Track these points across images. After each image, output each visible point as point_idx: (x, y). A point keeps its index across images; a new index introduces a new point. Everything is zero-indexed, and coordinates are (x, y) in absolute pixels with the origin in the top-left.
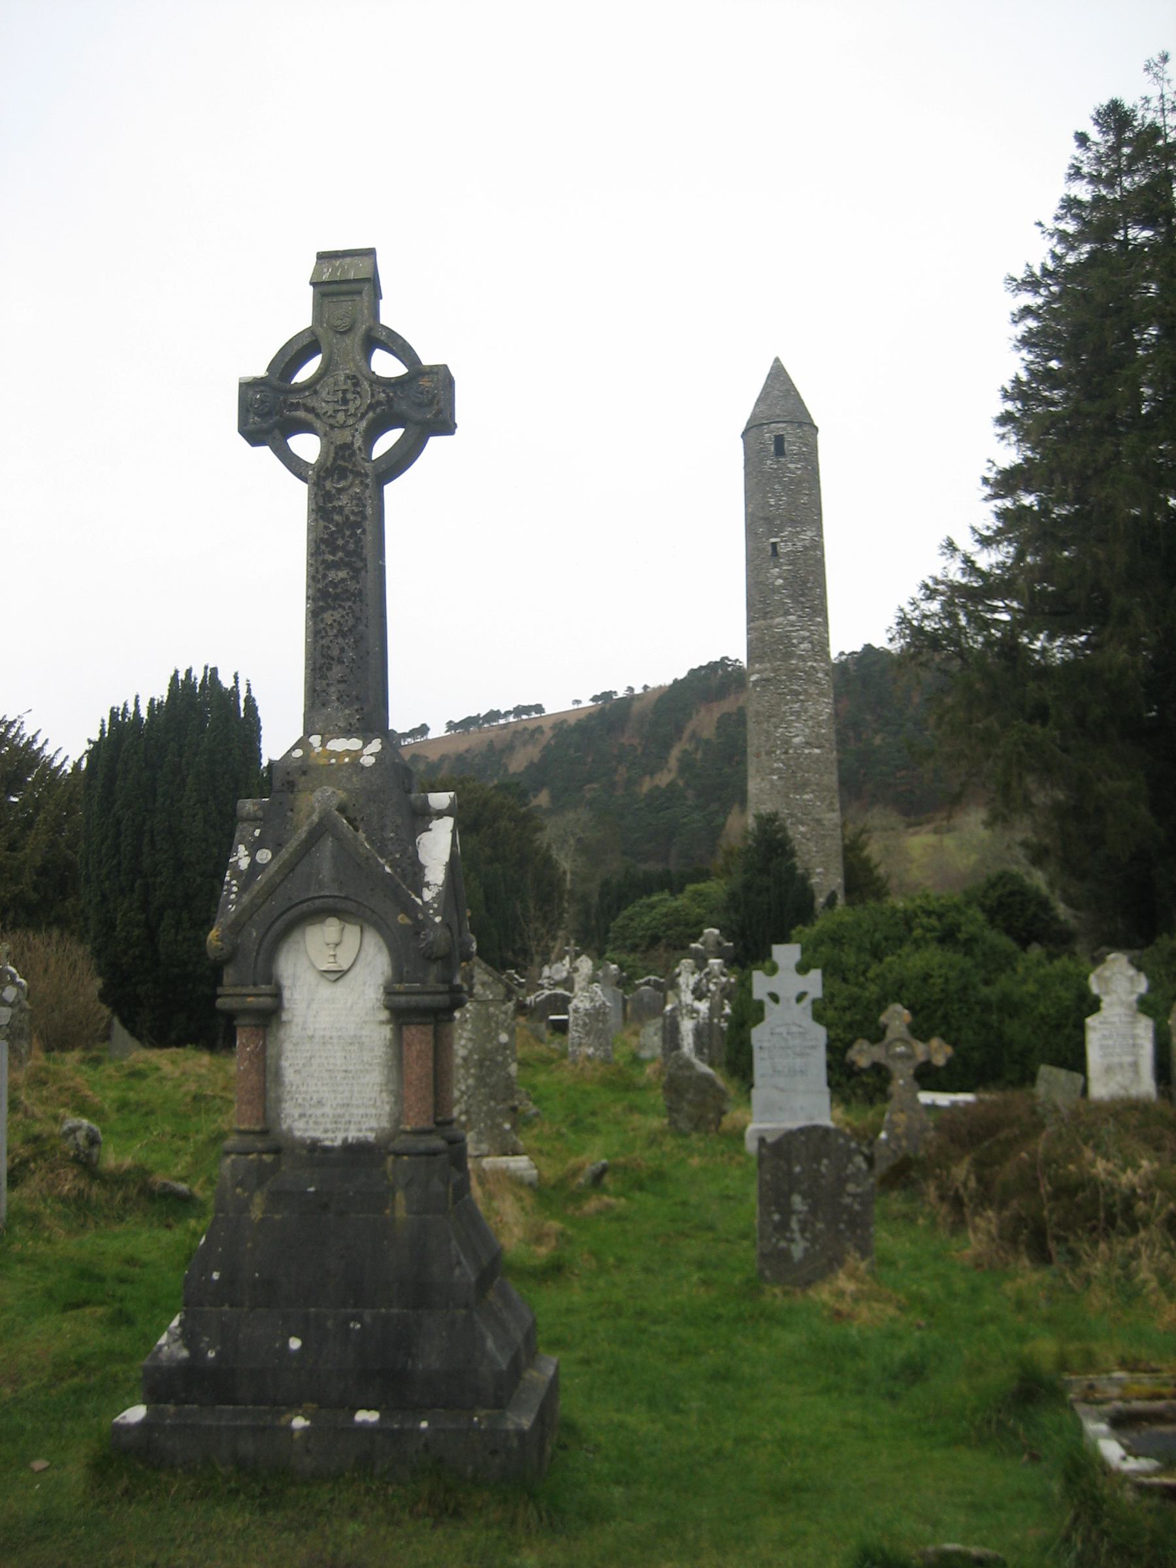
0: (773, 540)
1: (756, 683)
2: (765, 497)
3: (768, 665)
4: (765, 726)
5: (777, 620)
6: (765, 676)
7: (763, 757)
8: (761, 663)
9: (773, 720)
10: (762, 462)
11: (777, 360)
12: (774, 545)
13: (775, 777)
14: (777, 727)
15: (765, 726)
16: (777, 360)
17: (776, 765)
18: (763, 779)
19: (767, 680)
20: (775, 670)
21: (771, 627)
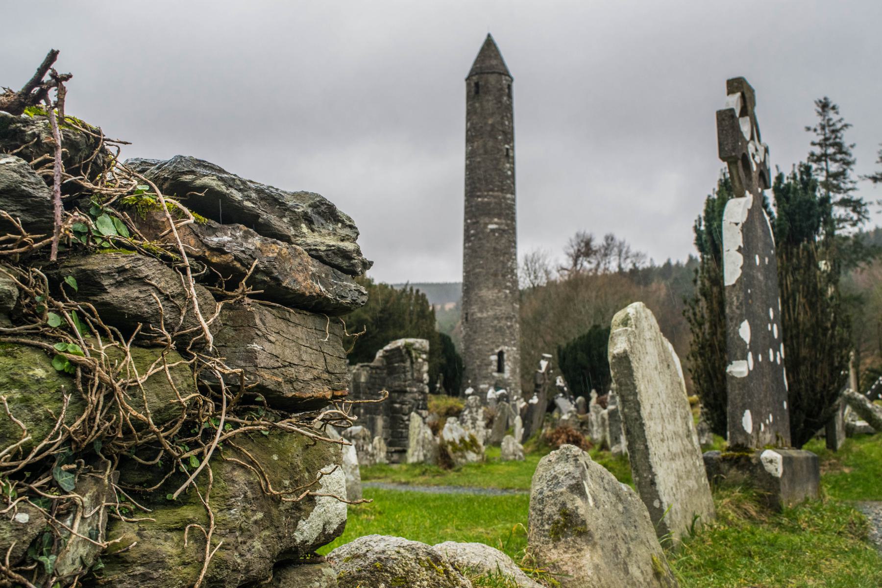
0: (507, 146)
1: (493, 231)
2: (502, 118)
3: (504, 221)
4: (501, 258)
5: (509, 196)
6: (503, 227)
7: (500, 277)
8: (499, 218)
9: (507, 256)
10: (501, 96)
11: (489, 36)
12: (507, 149)
13: (508, 291)
14: (508, 261)
15: (501, 258)
16: (489, 36)
17: (509, 284)
18: (499, 291)
19: (504, 231)
20: (507, 225)
21: (505, 198)
